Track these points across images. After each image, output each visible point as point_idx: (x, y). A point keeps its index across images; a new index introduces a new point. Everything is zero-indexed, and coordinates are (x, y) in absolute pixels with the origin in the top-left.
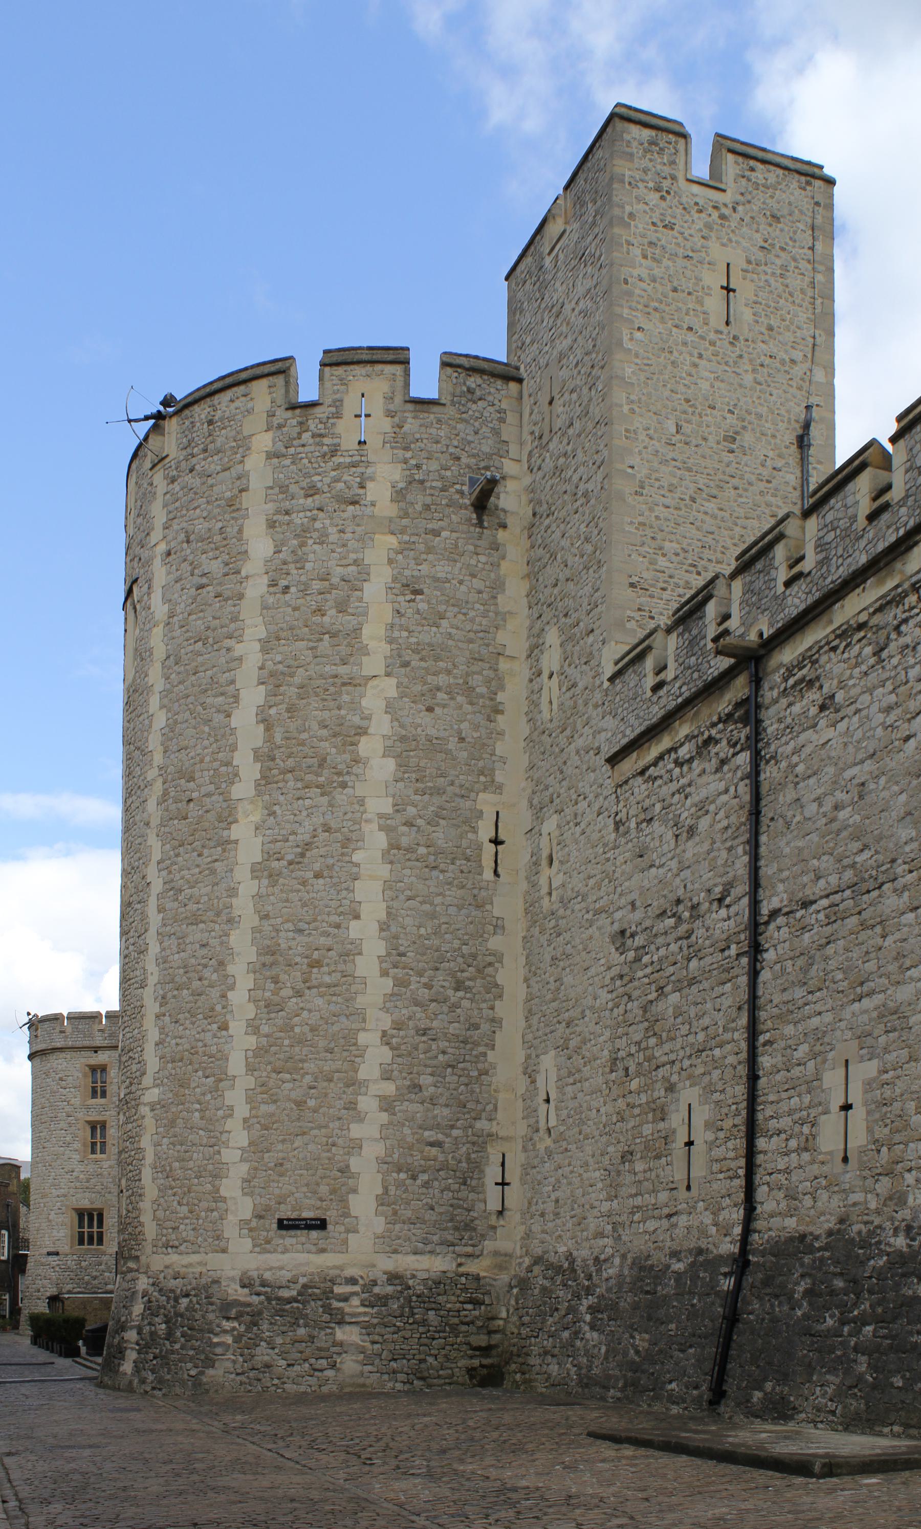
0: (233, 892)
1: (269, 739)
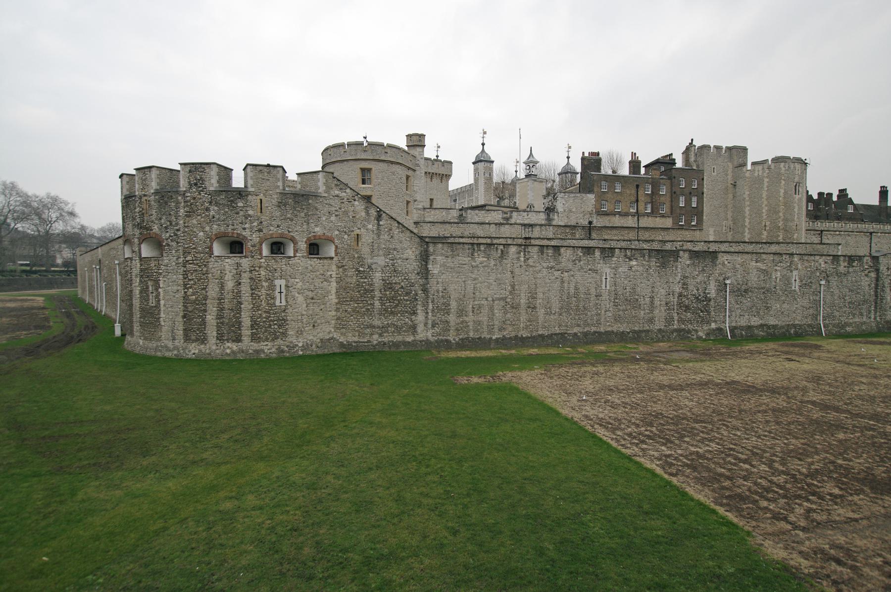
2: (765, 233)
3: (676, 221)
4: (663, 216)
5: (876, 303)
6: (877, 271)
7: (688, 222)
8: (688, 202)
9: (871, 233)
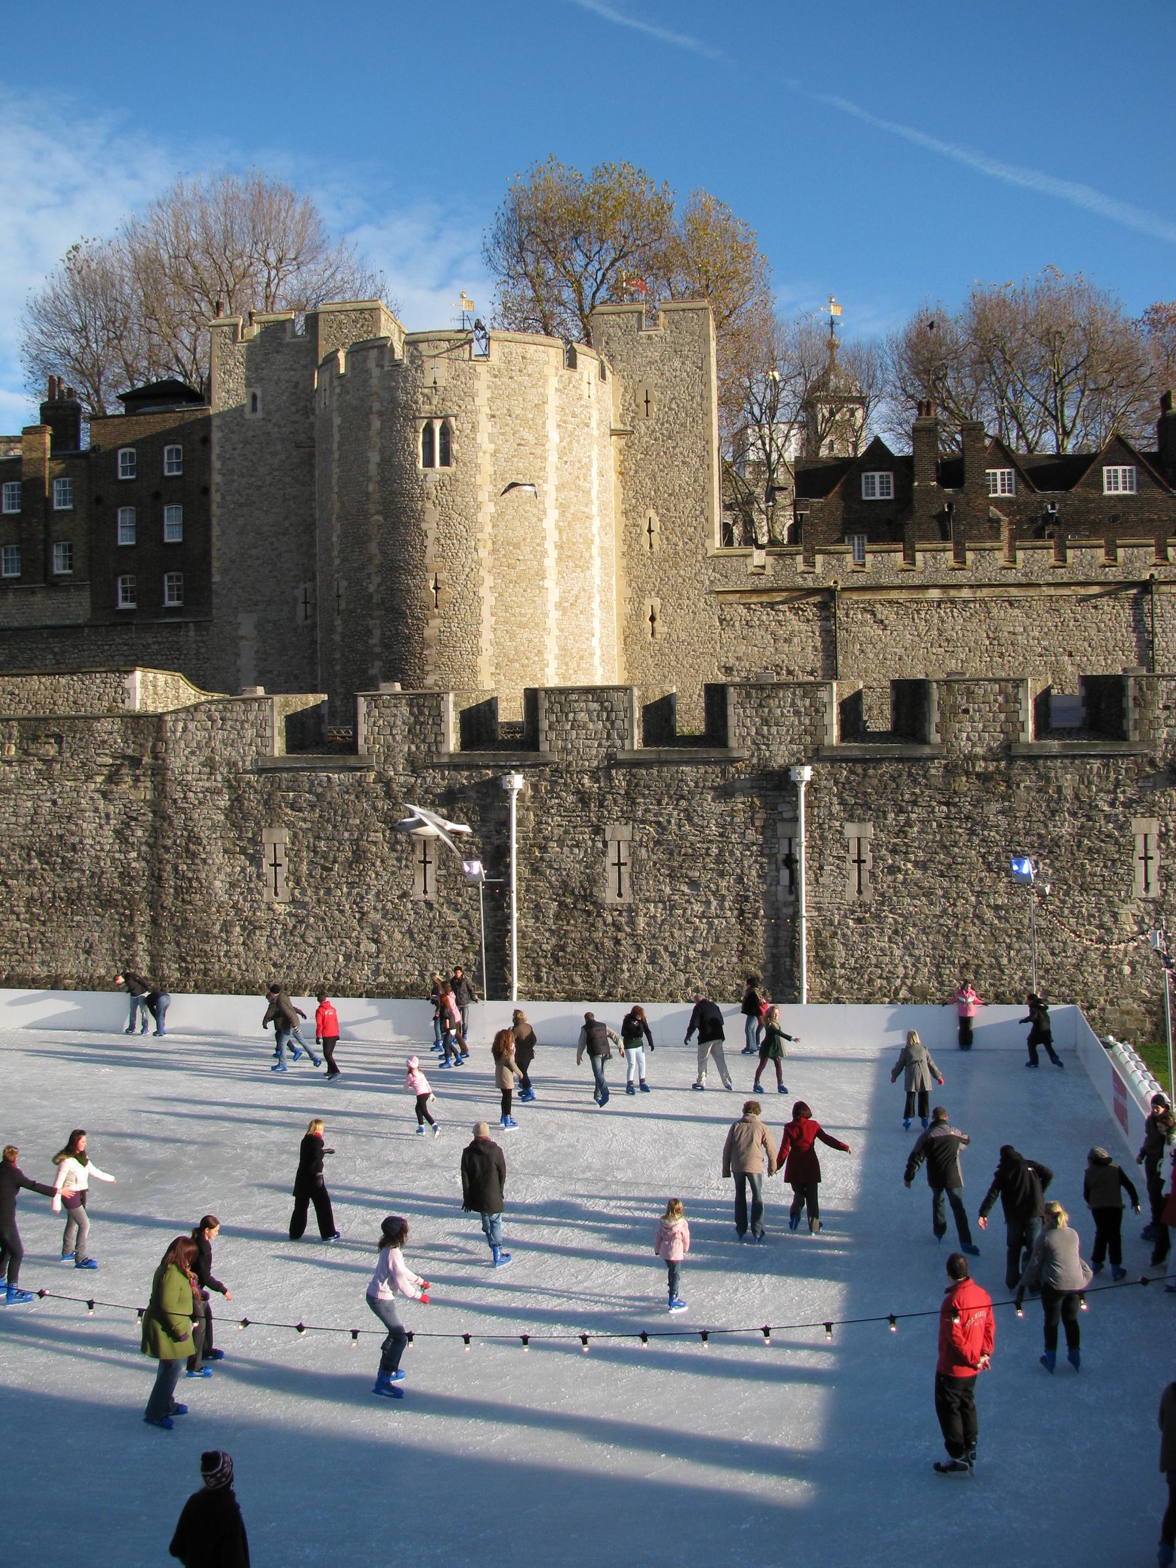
0: (546, 615)
1: (561, 538)
2: (338, 622)
3: (104, 602)
4: (53, 584)
5: (155, 904)
6: (159, 771)
7: (148, 597)
8: (149, 527)
9: (1146, 587)
